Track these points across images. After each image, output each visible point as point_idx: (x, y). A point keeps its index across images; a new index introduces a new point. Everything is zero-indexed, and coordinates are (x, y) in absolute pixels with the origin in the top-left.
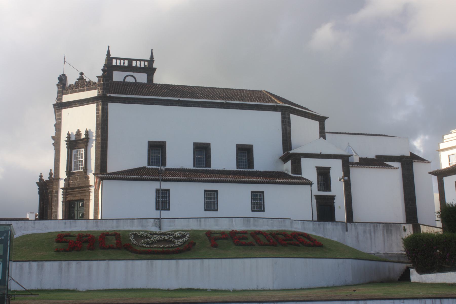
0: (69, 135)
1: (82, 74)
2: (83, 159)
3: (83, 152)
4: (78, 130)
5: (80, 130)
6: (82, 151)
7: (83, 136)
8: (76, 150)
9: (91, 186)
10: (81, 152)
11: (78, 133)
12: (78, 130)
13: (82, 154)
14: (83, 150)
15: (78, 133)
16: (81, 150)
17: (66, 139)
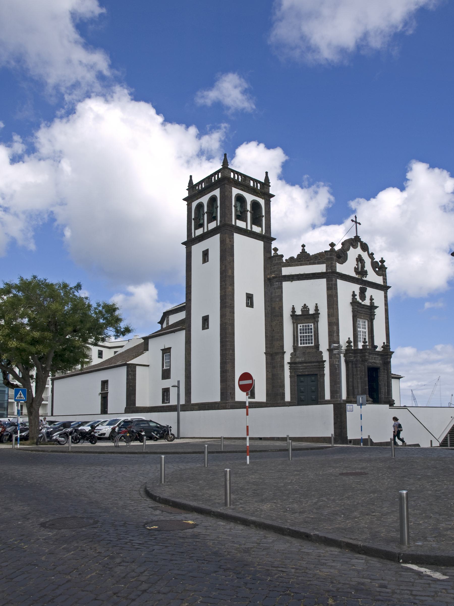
0: (293, 308)
1: (303, 246)
2: (313, 334)
3: (313, 327)
4: (305, 305)
5: (307, 305)
6: (311, 326)
7: (312, 312)
8: (301, 325)
9: (325, 361)
10: (310, 327)
11: (305, 308)
12: (305, 305)
13: (311, 329)
14: (312, 324)
15: (305, 308)
16: (310, 324)
17: (291, 314)
